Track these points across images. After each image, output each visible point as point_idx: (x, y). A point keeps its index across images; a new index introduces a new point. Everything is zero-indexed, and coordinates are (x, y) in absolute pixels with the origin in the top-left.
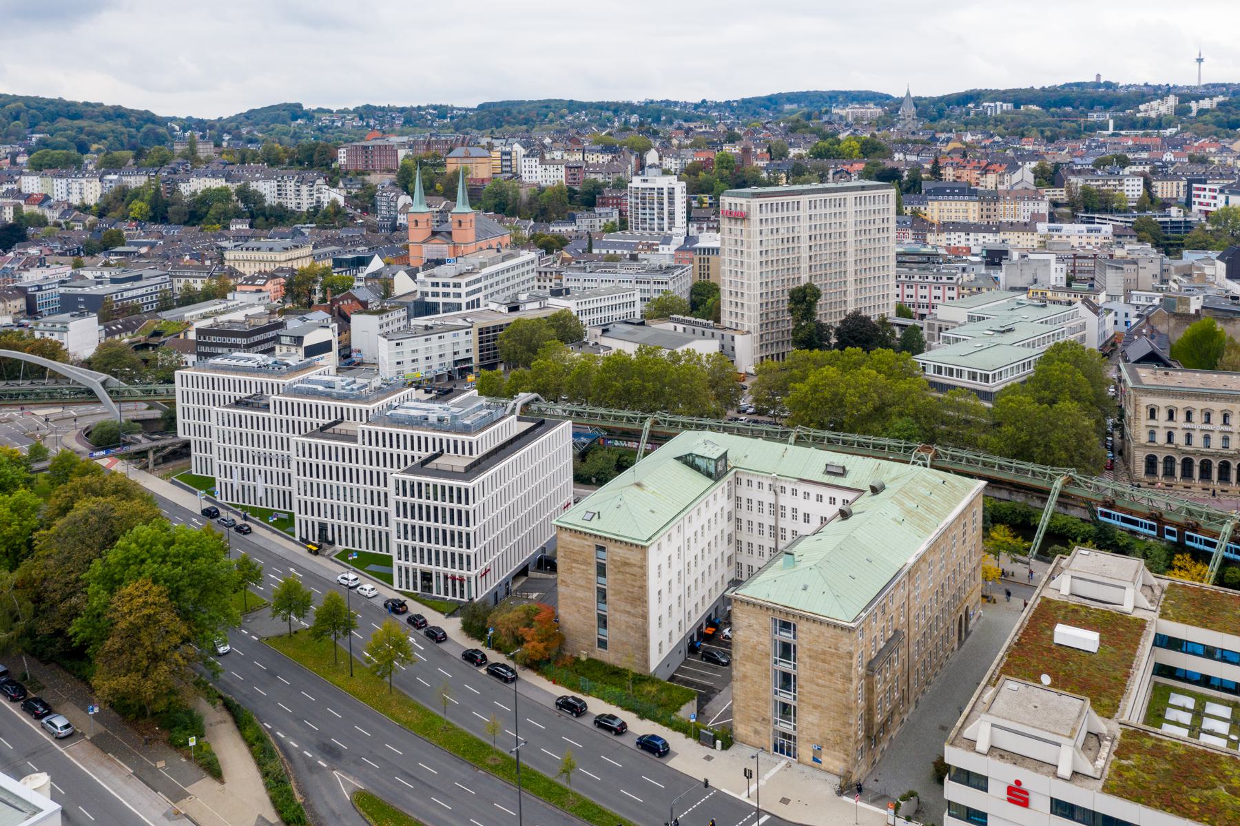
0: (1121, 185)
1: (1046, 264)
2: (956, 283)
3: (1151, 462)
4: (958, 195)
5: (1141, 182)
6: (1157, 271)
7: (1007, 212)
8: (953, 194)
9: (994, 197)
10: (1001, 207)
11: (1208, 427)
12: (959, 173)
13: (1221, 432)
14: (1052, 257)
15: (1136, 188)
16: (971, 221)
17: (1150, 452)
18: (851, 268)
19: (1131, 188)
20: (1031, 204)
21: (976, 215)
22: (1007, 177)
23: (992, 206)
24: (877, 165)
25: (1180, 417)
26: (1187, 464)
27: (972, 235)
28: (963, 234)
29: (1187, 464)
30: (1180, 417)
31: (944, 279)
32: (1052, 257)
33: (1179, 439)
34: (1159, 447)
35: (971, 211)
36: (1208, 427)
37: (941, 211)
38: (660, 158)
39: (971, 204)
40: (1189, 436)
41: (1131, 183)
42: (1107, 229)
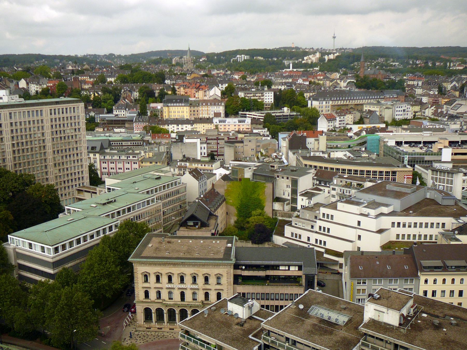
0: (263, 96)
1: (195, 144)
2: (138, 160)
3: (148, 312)
4: (179, 103)
5: (273, 94)
6: (254, 147)
7: (205, 112)
8: (176, 102)
9: (197, 104)
10: (201, 109)
11: (182, 286)
12: (187, 90)
13: (191, 289)
14: (198, 141)
15: (270, 97)
16: (186, 117)
17: (146, 306)
18: (50, 157)
19: (267, 97)
20: (215, 107)
21: (188, 114)
22: (207, 93)
23: (196, 109)
24: (148, 87)
25: (164, 279)
26: (172, 313)
27: (180, 125)
28: (175, 126)
29: (172, 313)
30: (164, 279)
31: (131, 157)
32: (198, 141)
33: (165, 295)
34: (154, 302)
35: (185, 112)
36: (182, 286)
37: (169, 112)
38: (27, 84)
39: (185, 108)
40: (170, 293)
41: (267, 95)
42: (248, 121)
